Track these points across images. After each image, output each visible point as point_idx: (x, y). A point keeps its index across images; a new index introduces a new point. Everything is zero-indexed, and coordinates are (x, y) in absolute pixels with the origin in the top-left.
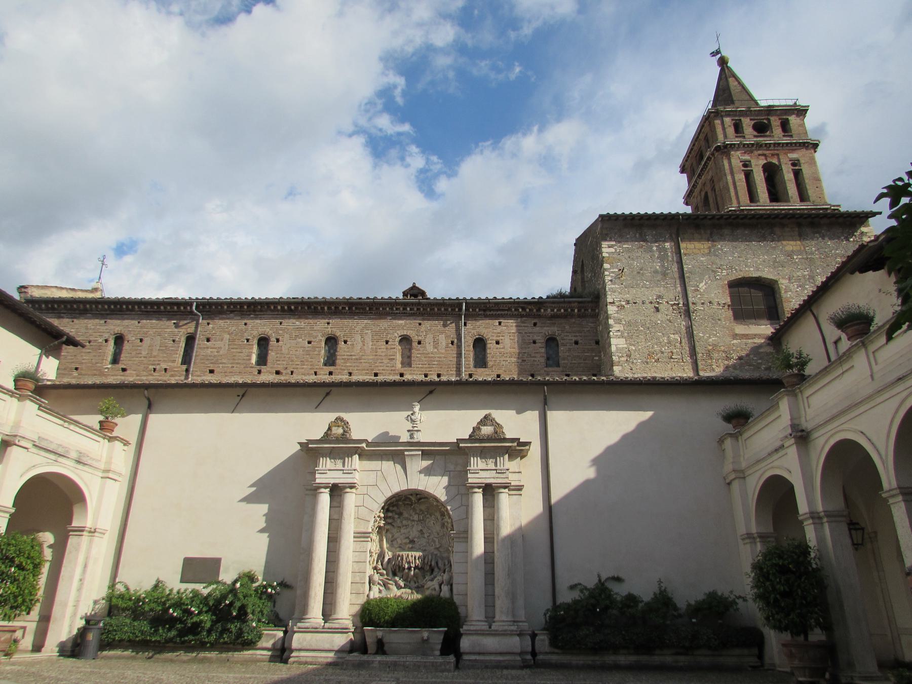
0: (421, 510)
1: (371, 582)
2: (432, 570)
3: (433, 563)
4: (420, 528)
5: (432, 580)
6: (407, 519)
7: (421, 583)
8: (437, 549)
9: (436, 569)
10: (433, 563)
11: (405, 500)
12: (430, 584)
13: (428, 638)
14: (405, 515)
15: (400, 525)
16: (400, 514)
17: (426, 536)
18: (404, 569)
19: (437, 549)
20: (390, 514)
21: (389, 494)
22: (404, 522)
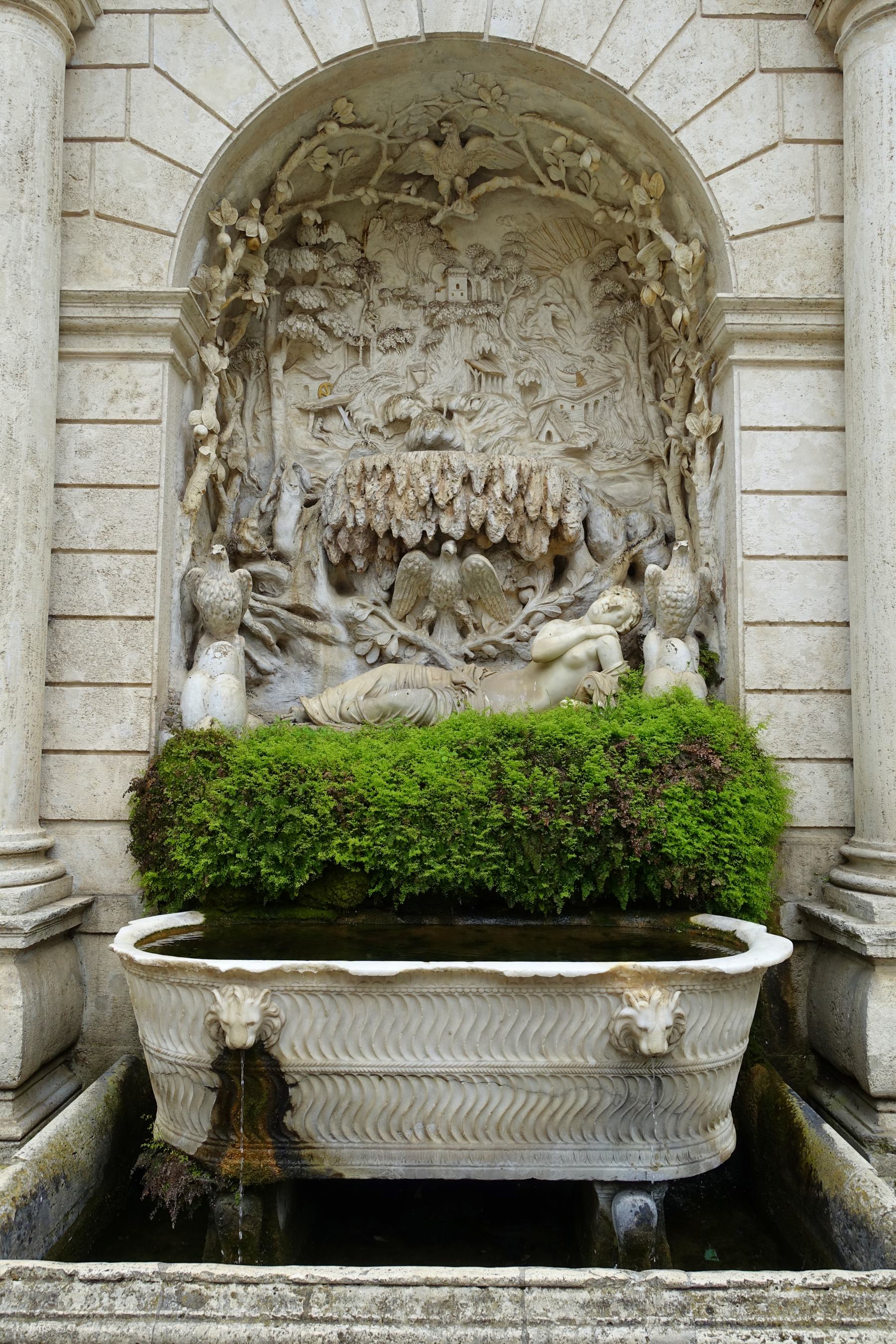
0: (483, 253)
1: (197, 625)
2: (560, 568)
3: (573, 519)
4: (484, 343)
5: (576, 608)
6: (404, 297)
7: (497, 632)
8: (579, 453)
9: (582, 557)
10: (573, 519)
11: (395, 179)
12: (553, 636)
13: (676, 1032)
14: (393, 275)
15: (366, 329)
16: (366, 268)
17: (509, 386)
18: (400, 548)
19: (579, 453)
20: (307, 261)
21: (297, 64)
22: (392, 314)
